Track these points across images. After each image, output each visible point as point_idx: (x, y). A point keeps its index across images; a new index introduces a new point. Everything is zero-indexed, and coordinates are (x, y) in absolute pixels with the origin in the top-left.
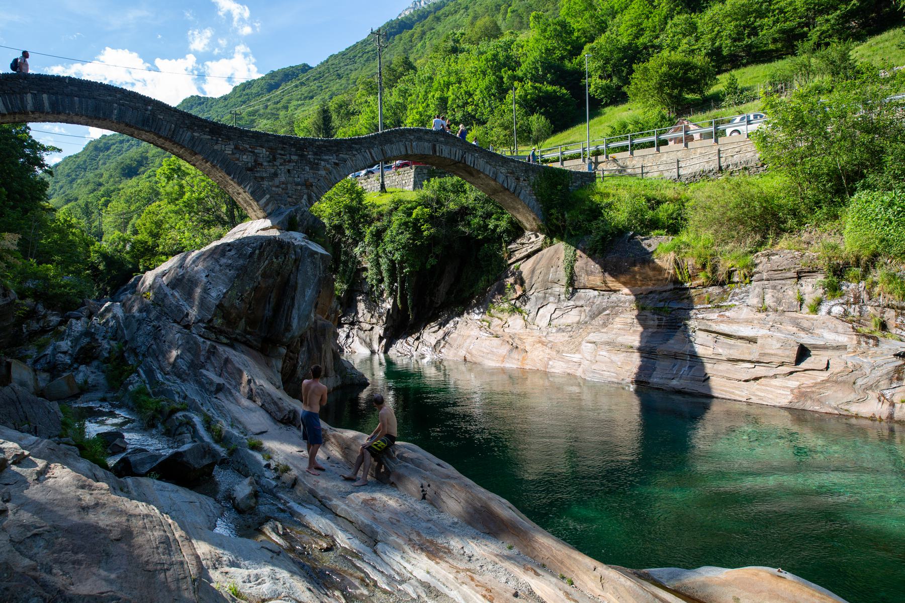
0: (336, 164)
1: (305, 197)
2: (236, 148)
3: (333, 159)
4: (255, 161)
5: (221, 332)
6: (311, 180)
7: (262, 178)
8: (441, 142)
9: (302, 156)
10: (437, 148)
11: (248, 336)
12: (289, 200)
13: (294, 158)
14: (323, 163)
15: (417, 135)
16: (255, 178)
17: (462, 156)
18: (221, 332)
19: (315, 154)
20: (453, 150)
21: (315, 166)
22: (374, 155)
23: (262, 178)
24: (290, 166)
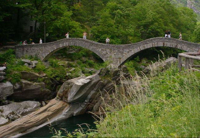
0: (128, 52)
1: (119, 62)
2: (102, 50)
3: (128, 50)
4: (106, 53)
5: (58, 98)
6: (121, 57)
7: (108, 57)
8: (167, 42)
9: (118, 50)
10: (165, 44)
11: (65, 100)
12: (114, 63)
13: (116, 51)
14: (124, 52)
15: (157, 40)
16: (106, 57)
17: (176, 46)
18: (58, 98)
19: (122, 49)
20: (172, 43)
21: (122, 53)
22: (141, 48)
23: (108, 57)
24: (115, 54)
